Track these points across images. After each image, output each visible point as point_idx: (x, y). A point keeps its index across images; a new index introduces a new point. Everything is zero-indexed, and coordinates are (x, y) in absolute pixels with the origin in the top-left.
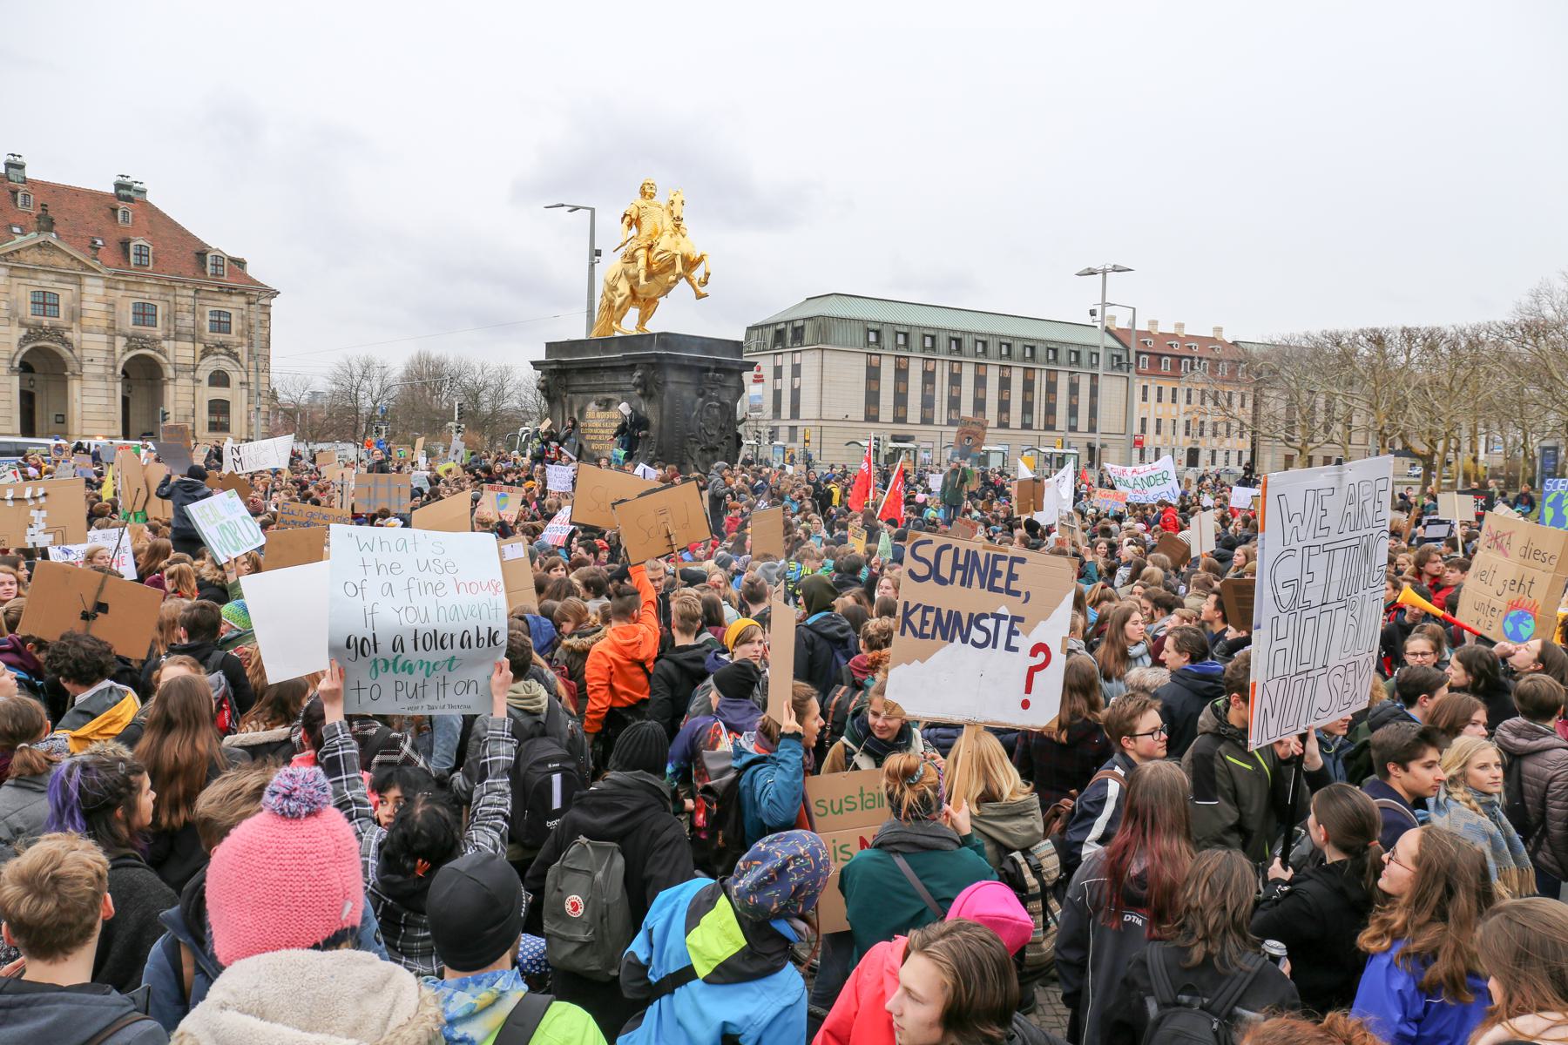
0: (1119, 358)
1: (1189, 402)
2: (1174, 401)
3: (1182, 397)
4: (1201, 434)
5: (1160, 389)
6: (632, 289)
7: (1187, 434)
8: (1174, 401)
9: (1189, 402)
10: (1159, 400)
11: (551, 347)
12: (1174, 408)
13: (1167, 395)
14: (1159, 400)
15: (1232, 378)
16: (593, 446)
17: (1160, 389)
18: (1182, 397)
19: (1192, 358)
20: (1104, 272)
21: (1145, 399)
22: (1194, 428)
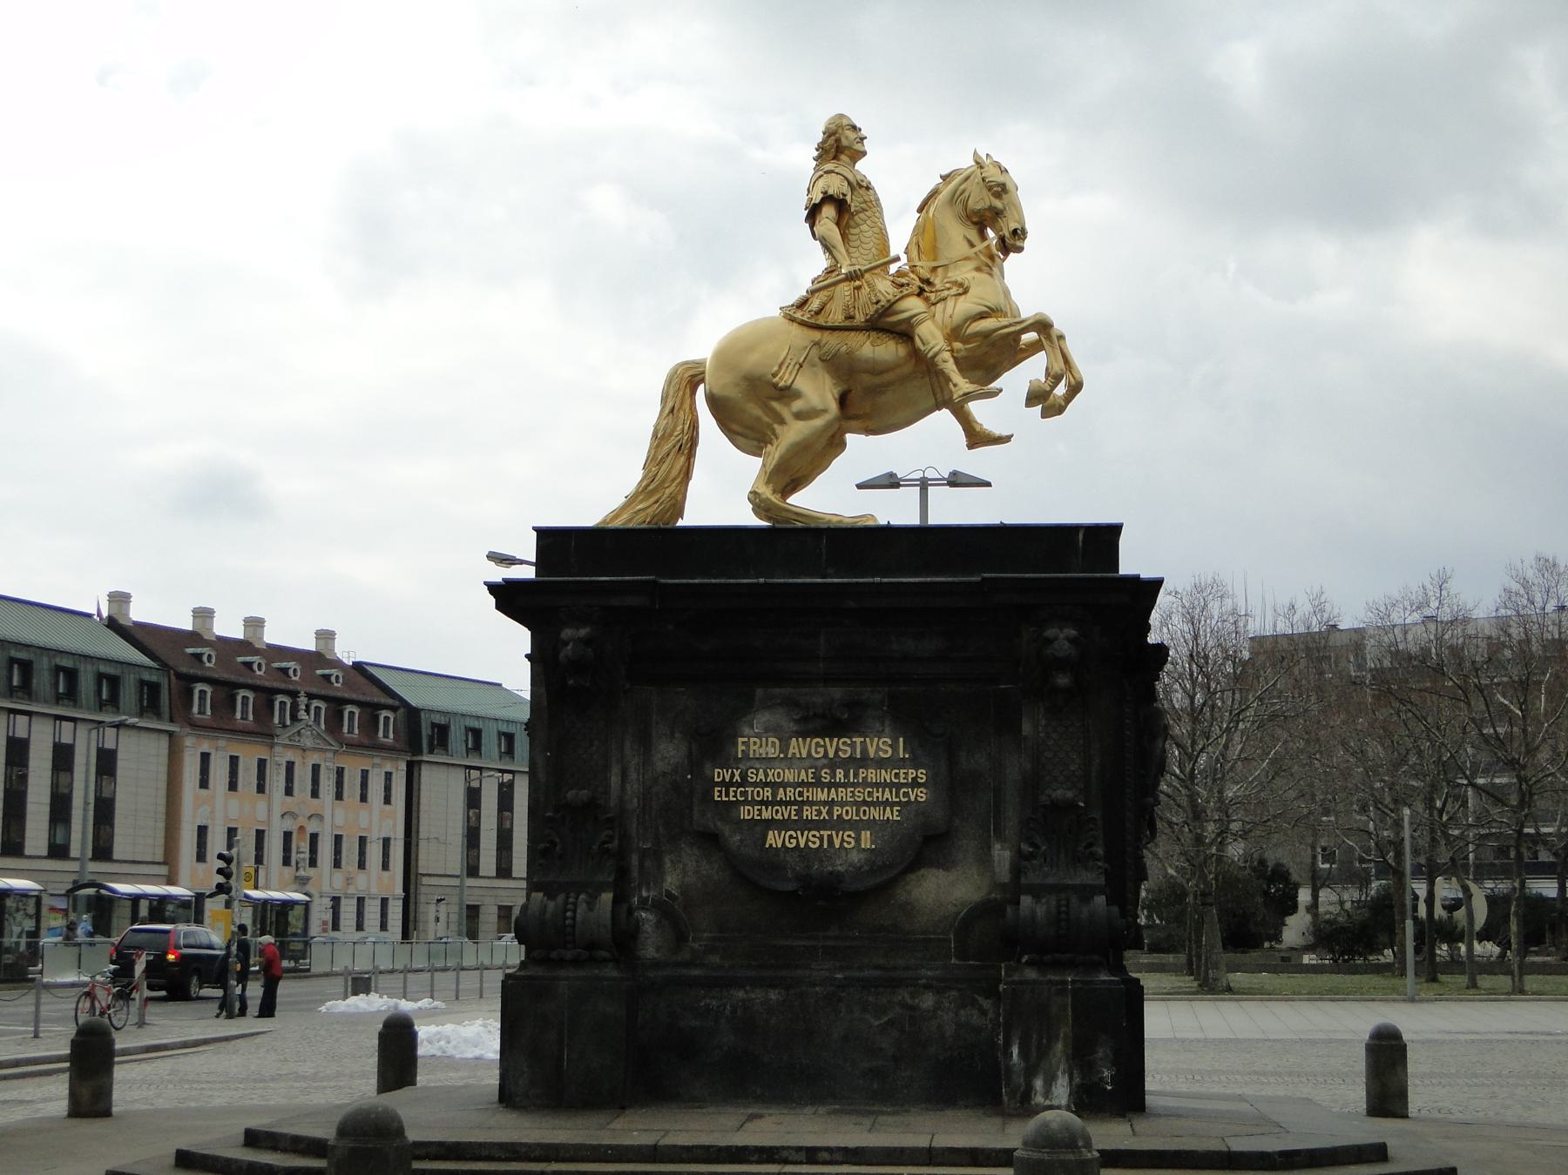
0: (154, 688)
1: (289, 791)
2: (261, 789)
3: (276, 780)
4: (313, 863)
5: (234, 761)
6: (843, 400)
7: (286, 861)
8: (261, 789)
9: (289, 791)
10: (233, 786)
11: (552, 541)
12: (261, 805)
13: (247, 776)
14: (233, 786)
15: (368, 745)
16: (774, 839)
17: (234, 761)
18: (276, 780)
19: (294, 694)
20: (924, 484)
21: (204, 783)
22: (301, 846)
